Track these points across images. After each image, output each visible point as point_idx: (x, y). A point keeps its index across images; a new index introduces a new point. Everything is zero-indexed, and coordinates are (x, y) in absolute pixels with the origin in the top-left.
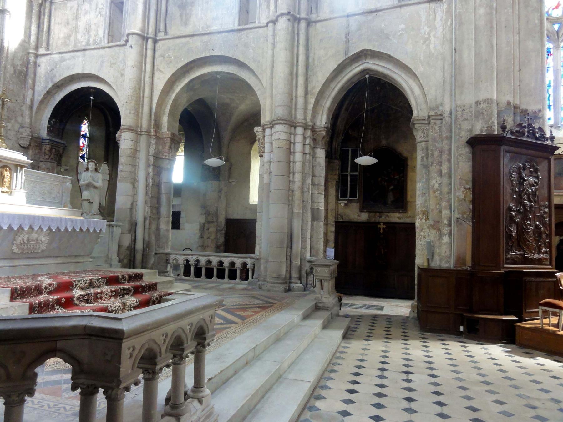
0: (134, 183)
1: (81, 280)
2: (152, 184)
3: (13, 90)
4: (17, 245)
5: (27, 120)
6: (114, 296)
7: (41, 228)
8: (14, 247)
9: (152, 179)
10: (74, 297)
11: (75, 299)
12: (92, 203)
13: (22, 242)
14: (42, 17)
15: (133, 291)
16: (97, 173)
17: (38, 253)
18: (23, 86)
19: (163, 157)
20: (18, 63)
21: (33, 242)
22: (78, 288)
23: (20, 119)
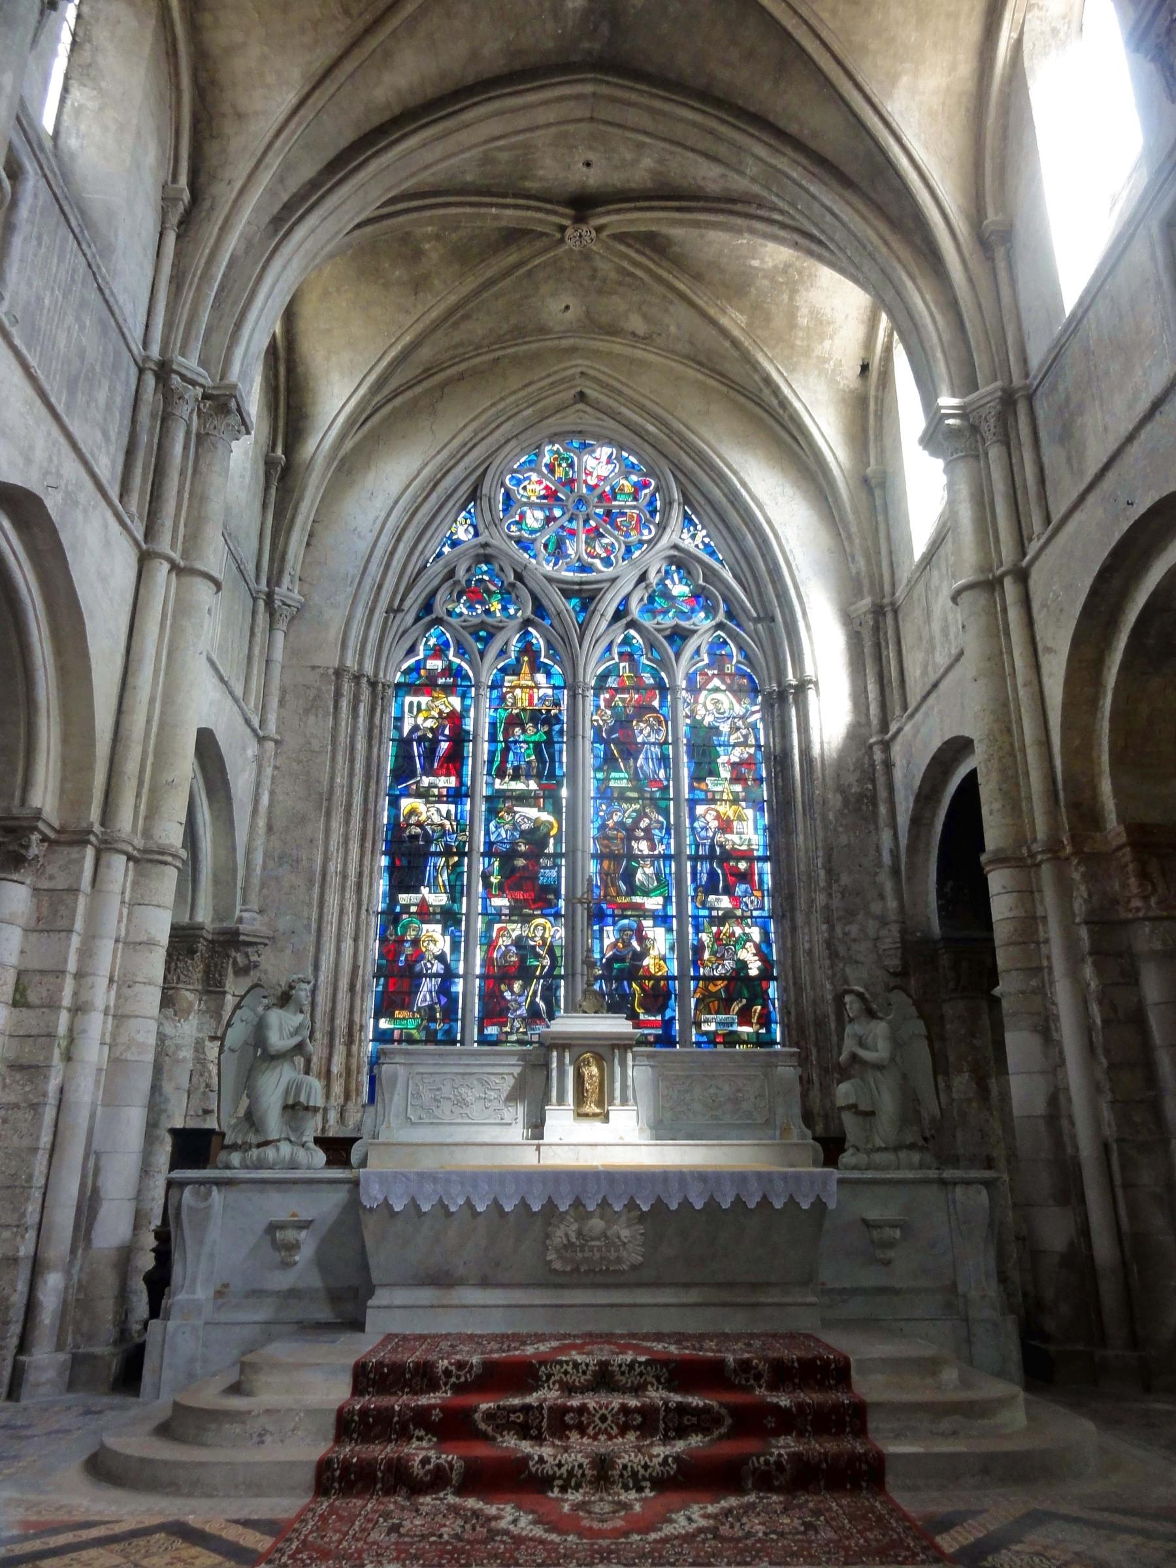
0: (1046, 1029)
1: (567, 1362)
2: (1103, 1021)
3: (848, 845)
4: (557, 1251)
5: (892, 904)
6: (636, 1428)
7: (604, 1204)
8: (551, 1256)
9: (1100, 1003)
10: (475, 1409)
11: (477, 1416)
12: (872, 1114)
13: (565, 1242)
14: (884, 653)
15: (729, 1421)
16: (874, 1023)
17: (623, 1272)
18: (872, 827)
19: (1130, 916)
20: (851, 778)
21: (598, 1243)
22: (557, 1386)
23: (876, 908)
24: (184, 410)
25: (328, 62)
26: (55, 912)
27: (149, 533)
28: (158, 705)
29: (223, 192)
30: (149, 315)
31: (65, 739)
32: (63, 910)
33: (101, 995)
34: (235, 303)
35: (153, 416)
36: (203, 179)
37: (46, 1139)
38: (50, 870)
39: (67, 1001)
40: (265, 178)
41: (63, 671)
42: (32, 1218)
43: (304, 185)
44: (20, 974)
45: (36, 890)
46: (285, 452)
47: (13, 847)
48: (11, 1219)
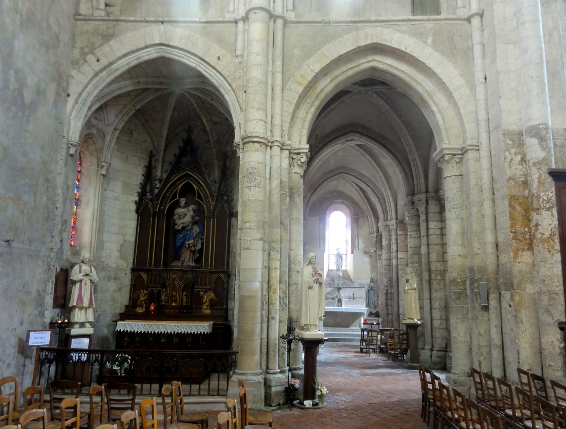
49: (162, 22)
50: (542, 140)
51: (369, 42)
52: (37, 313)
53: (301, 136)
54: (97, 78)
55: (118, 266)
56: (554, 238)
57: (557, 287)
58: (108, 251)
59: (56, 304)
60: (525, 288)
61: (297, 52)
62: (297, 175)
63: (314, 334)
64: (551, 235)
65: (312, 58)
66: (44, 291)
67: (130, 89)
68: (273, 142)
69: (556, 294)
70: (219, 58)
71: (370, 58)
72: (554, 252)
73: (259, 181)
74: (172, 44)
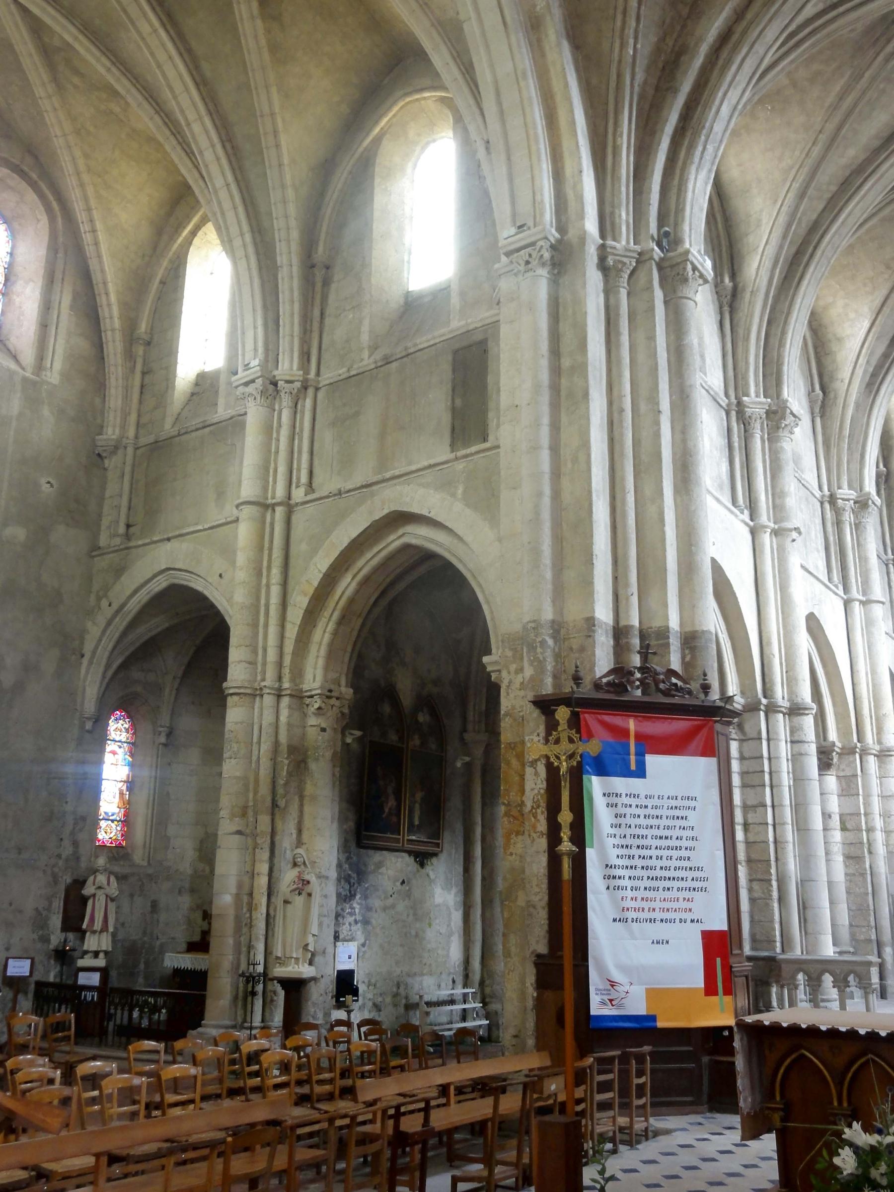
24: (848, 517)
25: (882, 299)
26: (849, 786)
27: (846, 589)
28: (869, 676)
29: (840, 387)
30: (818, 470)
31: (834, 704)
32: (853, 786)
33: (878, 823)
34: (858, 443)
35: (833, 524)
36: (826, 379)
37: (870, 889)
38: (842, 767)
39: (864, 827)
40: (860, 372)
41: (827, 674)
42: (873, 924)
43: (879, 359)
44: (841, 816)
45: (837, 776)
46: (885, 466)
47: (825, 760)
48: (865, 924)
49: (169, 539)
50: (532, 648)
51: (386, 511)
52: (35, 936)
53: (315, 668)
54: (112, 627)
55: (195, 872)
56: (536, 813)
57: (536, 894)
58: (178, 850)
59: (65, 928)
60: (517, 897)
61: (304, 547)
62: (315, 728)
63: (290, 972)
64: (533, 807)
65: (320, 552)
66: (49, 909)
67: (166, 625)
68: (261, 689)
69: (534, 907)
70: (221, 576)
71: (400, 532)
72: (534, 835)
73: (236, 749)
74: (177, 567)
